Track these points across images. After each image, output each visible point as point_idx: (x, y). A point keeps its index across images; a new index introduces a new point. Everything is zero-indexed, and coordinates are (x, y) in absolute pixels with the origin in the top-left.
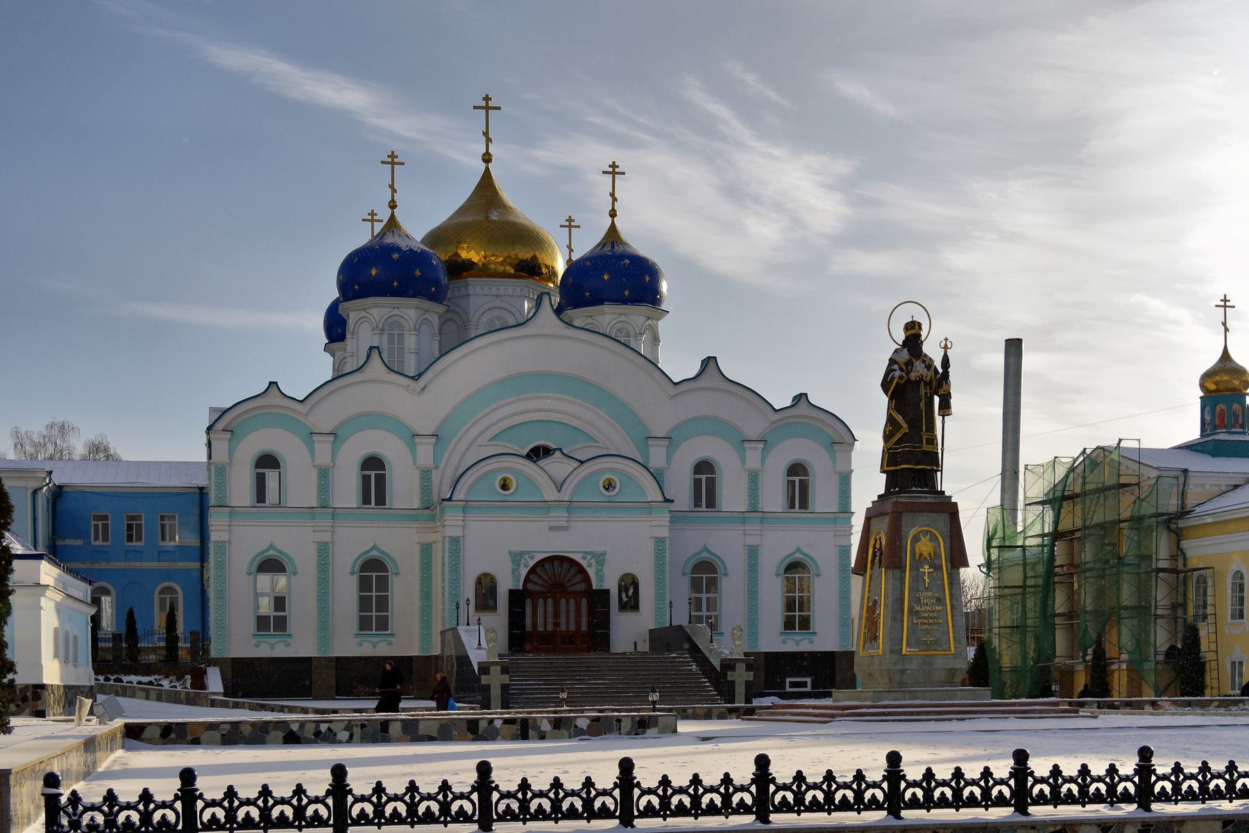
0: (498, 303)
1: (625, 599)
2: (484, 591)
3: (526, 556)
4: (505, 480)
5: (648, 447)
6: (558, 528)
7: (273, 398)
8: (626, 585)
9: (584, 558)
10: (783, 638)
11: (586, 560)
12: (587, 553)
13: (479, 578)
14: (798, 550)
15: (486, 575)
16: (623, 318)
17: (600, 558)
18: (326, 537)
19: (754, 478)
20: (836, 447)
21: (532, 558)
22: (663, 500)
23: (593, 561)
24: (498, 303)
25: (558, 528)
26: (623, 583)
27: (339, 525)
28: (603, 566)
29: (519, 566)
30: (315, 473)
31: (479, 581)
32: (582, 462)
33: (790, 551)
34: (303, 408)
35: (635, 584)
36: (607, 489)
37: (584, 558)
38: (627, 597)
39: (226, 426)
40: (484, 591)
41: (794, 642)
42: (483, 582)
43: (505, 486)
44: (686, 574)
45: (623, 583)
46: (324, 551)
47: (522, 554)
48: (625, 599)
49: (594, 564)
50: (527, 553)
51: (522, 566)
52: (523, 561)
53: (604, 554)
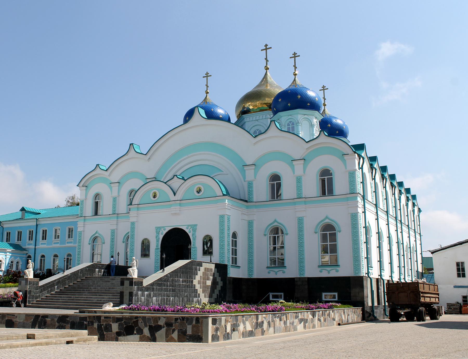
0: (257, 123)
1: (206, 249)
2: (145, 247)
3: (162, 229)
4: (155, 193)
5: (245, 171)
6: (175, 214)
7: (98, 171)
8: (206, 241)
9: (187, 228)
10: (320, 269)
11: (189, 229)
12: (189, 226)
13: (143, 241)
14: (327, 217)
15: (146, 239)
16: (290, 117)
17: (194, 227)
18: (115, 227)
19: (299, 180)
20: (346, 157)
21: (165, 230)
22: (222, 195)
23: (191, 230)
24: (257, 123)
25: (175, 214)
26: (205, 240)
27: (120, 221)
28: (195, 232)
29: (159, 234)
30: (112, 199)
31: (143, 243)
32: (185, 180)
33: (322, 219)
34: (107, 173)
35: (211, 241)
36: (198, 192)
37: (187, 228)
38: (207, 248)
39: (83, 185)
40: (145, 247)
41: (327, 272)
42: (144, 243)
43: (155, 197)
44: (266, 235)
45: (205, 240)
46: (113, 233)
47: (160, 228)
48: (206, 249)
49: (192, 231)
50: (163, 227)
51: (160, 233)
52: (161, 232)
53: (196, 225)
